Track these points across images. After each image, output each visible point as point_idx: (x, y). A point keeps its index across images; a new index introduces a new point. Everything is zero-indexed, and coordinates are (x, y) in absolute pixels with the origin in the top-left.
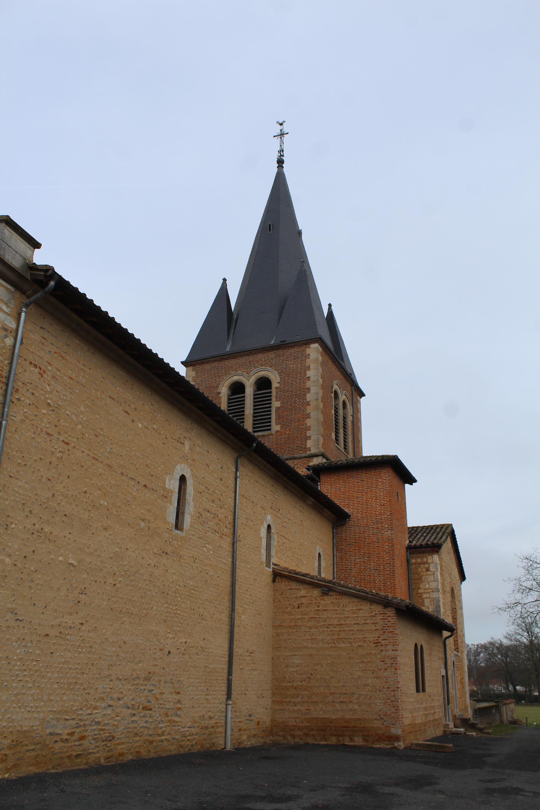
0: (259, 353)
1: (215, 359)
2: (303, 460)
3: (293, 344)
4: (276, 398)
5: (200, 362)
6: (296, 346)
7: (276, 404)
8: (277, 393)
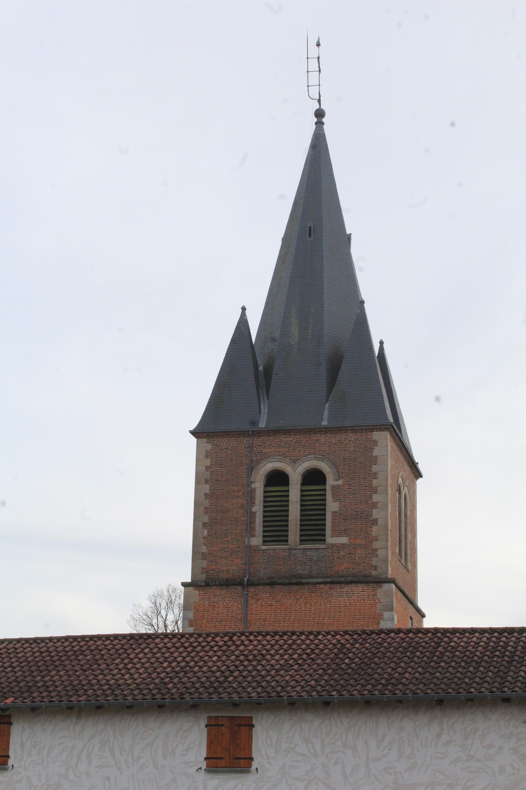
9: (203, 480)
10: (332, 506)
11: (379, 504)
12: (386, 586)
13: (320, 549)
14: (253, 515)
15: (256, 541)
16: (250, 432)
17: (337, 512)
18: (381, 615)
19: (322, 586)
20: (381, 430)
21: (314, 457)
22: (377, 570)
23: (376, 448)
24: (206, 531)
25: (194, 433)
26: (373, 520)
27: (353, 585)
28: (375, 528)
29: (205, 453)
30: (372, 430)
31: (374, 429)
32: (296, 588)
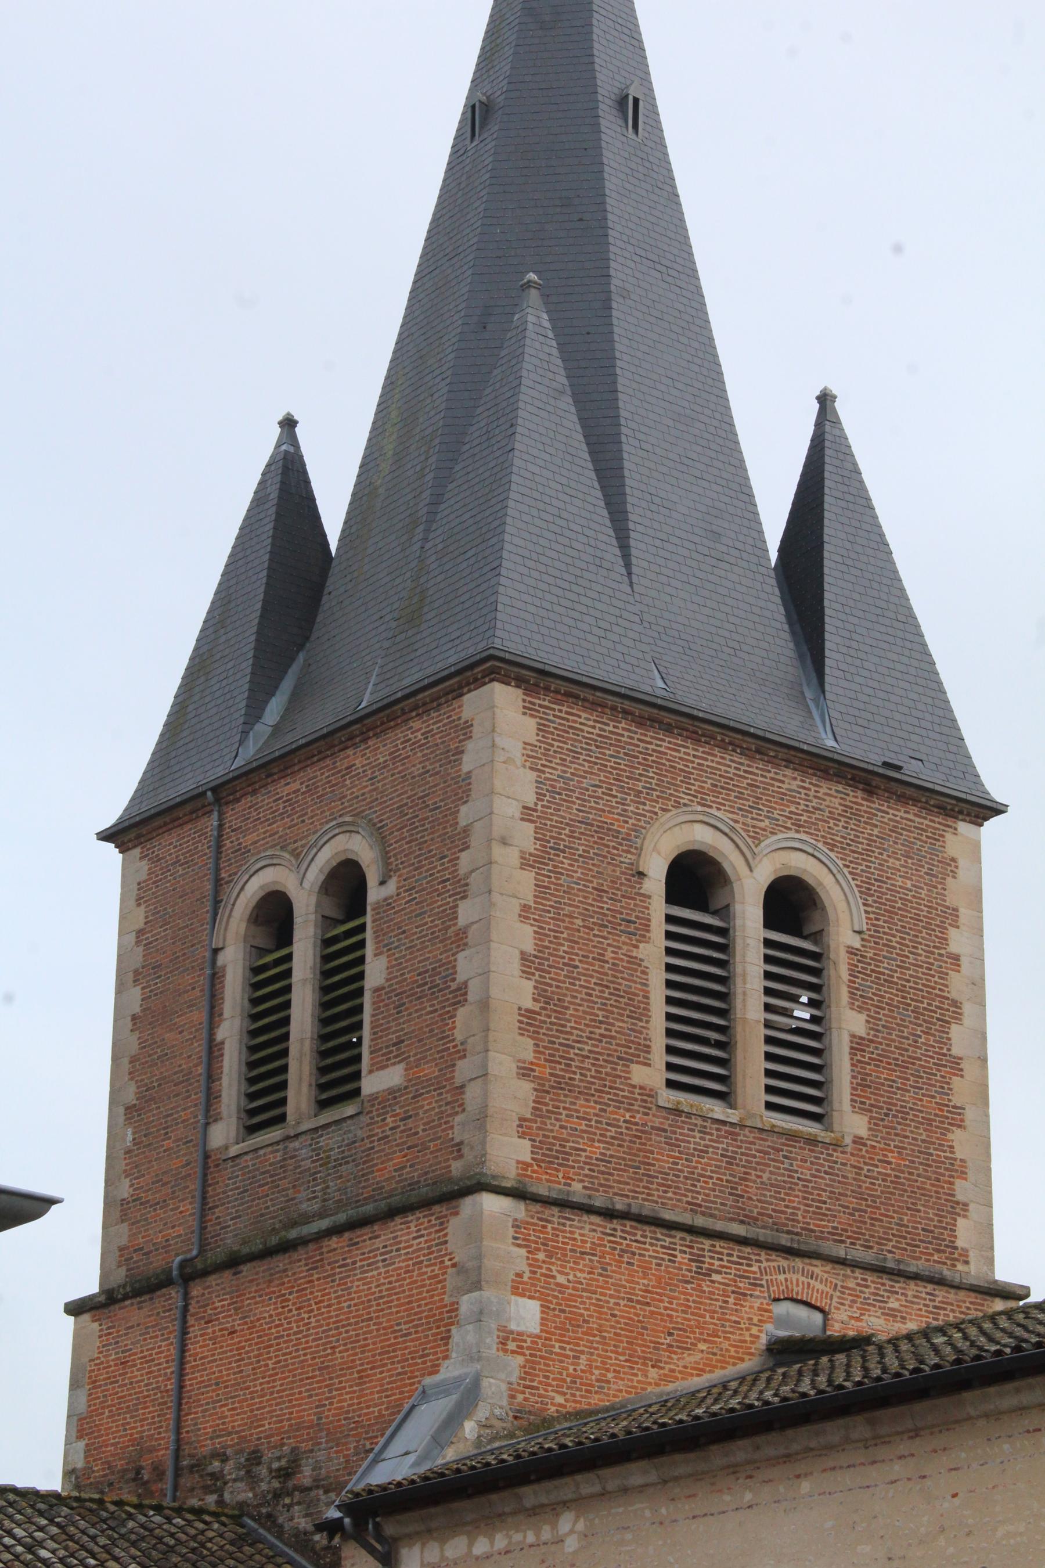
1: (627, 705)
2: (962, 1294)
3: (909, 792)
5: (564, 687)
6: (916, 801)
7: (849, 1022)
9: (131, 975)
10: (376, 971)
11: (471, 933)
12: (467, 1204)
13: (345, 1119)
14: (213, 1050)
15: (223, 1134)
16: (209, 793)
17: (383, 988)
18: (454, 1308)
19: (334, 1242)
20: (478, 683)
21: (339, 825)
22: (461, 1156)
23: (470, 745)
24: (130, 1131)
26: (459, 989)
27: (398, 1220)
28: (462, 1013)
29: (136, 892)
30: (457, 693)
31: (461, 687)
32: (280, 1262)
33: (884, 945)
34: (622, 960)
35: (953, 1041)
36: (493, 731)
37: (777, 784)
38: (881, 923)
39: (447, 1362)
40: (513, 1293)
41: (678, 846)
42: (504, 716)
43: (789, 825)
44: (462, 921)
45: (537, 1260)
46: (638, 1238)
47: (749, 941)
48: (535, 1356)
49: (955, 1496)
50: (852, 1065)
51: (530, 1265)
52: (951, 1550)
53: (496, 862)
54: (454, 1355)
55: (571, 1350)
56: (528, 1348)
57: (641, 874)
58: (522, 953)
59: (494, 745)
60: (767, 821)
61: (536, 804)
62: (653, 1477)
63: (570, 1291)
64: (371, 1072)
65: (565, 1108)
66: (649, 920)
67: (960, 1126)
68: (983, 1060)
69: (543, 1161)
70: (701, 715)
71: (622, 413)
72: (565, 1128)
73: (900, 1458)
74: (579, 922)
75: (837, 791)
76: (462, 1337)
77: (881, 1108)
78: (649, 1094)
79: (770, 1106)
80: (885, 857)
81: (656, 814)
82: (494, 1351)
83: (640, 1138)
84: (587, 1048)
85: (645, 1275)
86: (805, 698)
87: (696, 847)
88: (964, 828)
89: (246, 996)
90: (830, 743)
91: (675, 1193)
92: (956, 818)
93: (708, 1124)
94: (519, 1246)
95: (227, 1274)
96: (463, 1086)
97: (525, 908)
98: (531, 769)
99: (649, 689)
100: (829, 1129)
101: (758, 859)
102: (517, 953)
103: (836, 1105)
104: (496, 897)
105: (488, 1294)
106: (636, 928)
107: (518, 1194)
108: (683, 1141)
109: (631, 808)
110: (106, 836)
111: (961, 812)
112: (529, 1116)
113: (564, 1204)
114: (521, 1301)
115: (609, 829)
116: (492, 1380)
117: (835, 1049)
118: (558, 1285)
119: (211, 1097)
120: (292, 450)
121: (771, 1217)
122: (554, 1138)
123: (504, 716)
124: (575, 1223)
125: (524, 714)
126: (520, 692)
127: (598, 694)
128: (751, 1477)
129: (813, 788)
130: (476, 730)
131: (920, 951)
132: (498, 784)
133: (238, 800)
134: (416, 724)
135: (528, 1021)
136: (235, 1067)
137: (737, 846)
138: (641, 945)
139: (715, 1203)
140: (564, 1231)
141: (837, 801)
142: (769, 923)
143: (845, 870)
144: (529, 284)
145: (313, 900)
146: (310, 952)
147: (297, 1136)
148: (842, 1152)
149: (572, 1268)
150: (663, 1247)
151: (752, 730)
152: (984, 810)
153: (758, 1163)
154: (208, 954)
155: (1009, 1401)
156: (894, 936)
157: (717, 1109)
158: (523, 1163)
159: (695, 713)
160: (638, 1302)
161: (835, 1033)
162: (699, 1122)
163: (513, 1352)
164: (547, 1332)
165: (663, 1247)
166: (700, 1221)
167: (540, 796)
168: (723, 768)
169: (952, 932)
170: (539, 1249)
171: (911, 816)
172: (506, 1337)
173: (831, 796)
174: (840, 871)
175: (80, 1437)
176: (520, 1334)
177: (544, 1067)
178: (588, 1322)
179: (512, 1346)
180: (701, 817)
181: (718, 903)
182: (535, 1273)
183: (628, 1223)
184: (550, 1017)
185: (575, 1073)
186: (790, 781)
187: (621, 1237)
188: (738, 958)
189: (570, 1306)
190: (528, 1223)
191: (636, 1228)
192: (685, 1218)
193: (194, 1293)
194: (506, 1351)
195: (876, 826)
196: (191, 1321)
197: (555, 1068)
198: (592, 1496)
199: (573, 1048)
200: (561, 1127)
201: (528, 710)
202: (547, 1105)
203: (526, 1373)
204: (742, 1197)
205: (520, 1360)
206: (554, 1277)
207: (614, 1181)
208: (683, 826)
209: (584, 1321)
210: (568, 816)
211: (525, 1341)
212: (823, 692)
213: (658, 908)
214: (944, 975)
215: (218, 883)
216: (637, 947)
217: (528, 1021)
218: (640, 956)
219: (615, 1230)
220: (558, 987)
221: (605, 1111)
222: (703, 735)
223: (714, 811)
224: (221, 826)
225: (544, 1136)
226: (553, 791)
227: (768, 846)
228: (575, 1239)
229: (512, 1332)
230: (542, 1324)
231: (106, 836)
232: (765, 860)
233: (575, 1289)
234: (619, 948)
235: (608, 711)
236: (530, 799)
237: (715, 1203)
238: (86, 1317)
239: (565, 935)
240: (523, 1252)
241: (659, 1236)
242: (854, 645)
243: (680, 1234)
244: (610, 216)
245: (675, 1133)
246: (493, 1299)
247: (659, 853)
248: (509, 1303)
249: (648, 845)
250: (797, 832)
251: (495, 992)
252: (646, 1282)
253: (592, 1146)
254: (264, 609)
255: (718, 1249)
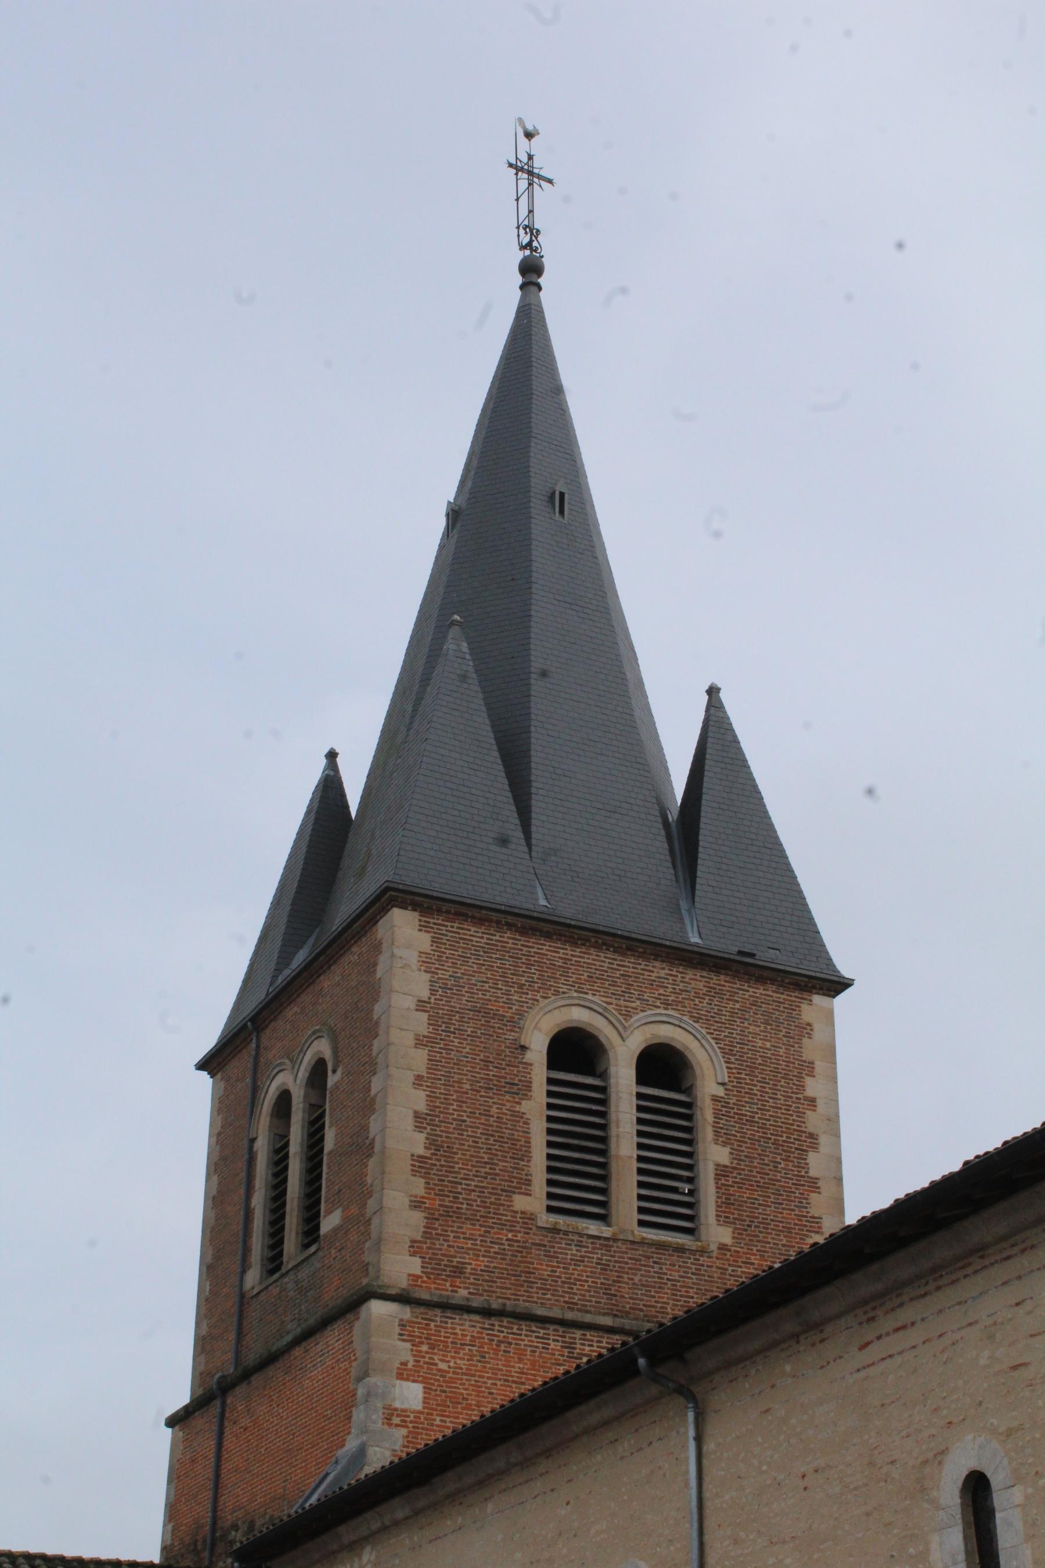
0: (657, 957)
1: (510, 919)
3: (765, 974)
4: (717, 1133)
6: (773, 981)
7: (713, 1153)
8: (716, 1116)
15: (252, 1277)
16: (249, 1024)
19: (297, 1352)
20: (385, 910)
25: (209, 1064)
30: (374, 921)
31: (376, 916)
32: (271, 1371)
33: (746, 1093)
34: (506, 1114)
35: (810, 1165)
36: (393, 944)
37: (647, 973)
38: (743, 1076)
39: (350, 1437)
40: (398, 1378)
41: (558, 1025)
42: (404, 932)
43: (658, 1004)
44: (373, 1092)
45: (420, 1351)
46: (515, 1331)
47: (621, 1095)
48: (418, 1428)
49: (568, 1503)
50: (717, 1188)
51: (414, 1356)
52: (565, 1551)
53: (393, 1044)
54: (353, 1431)
55: (451, 1422)
56: (411, 1422)
57: (524, 1048)
58: (415, 1112)
59: (393, 955)
60: (638, 1003)
61: (430, 998)
62: (407, 1511)
63: (451, 1375)
64: (325, 1217)
65: (452, 1231)
66: (531, 1082)
67: (818, 1233)
68: (839, 1180)
69: (432, 1274)
70: (573, 923)
71: (533, 711)
72: (453, 1247)
73: (541, 1475)
74: (467, 1086)
75: (701, 976)
76: (358, 1415)
77: (744, 1221)
78: (529, 1218)
79: (642, 1223)
80: (746, 1025)
81: (537, 1001)
82: (379, 1425)
83: (521, 1252)
84: (473, 1183)
85: (520, 1360)
86: (679, 909)
87: (574, 1025)
88: (818, 999)
89: (270, 1172)
90: (695, 939)
91: (553, 1295)
92: (811, 992)
93: (584, 1239)
94: (404, 1340)
95: (244, 1386)
96: (370, 1219)
97: (419, 1077)
98: (426, 971)
99: (531, 907)
100: (698, 1240)
101: (629, 1031)
102: (411, 1112)
103: (703, 1220)
104: (393, 1071)
105: (371, 1380)
106: (519, 1089)
107: (403, 1298)
108: (561, 1253)
109: (515, 998)
110: (202, 1066)
111: (814, 987)
112: (419, 1238)
113: (445, 1306)
114: (405, 1384)
115: (494, 1014)
116: (377, 1449)
117: (702, 1176)
118: (439, 1370)
119: (246, 1251)
120: (332, 773)
121: (642, 1310)
122: (443, 1255)
123: (404, 932)
124: (457, 1321)
125: (420, 930)
126: (416, 914)
127: (483, 912)
128: (461, 1504)
129: (680, 975)
130: (385, 945)
131: (779, 1096)
132: (396, 984)
133: (267, 1026)
134: (354, 949)
135: (420, 1165)
136: (261, 1225)
137: (610, 1022)
138: (524, 1102)
139: (590, 1301)
140: (447, 1328)
141: (701, 984)
142: (641, 1080)
143: (708, 1037)
144: (453, 623)
145: (302, 1092)
146: (299, 1132)
147: (287, 1272)
148: (708, 1257)
149: (453, 1357)
150: (537, 1337)
151: (619, 932)
152: (837, 985)
153: (630, 1268)
154: (245, 1143)
155: (594, 1419)
156: (755, 1086)
157: (593, 1228)
158: (413, 1275)
159: (597, 928)
160: (514, 1382)
161: (701, 1163)
162: (576, 1238)
163: (397, 1425)
164: (429, 1409)
165: (537, 1337)
166: (570, 1316)
167: (433, 991)
168: (598, 963)
169: (809, 1081)
170: (422, 1343)
171: (769, 993)
172: (390, 1414)
173: (696, 980)
174: (704, 1037)
175: (170, 1521)
176: (403, 1410)
177: (434, 1199)
178: (467, 1399)
179: (396, 1420)
180: (577, 1002)
181: (600, 1069)
182: (418, 1361)
183: (505, 1320)
184: (439, 1160)
185: (462, 1203)
186: (659, 970)
187: (499, 1331)
188: (613, 1108)
189: (450, 1387)
190: (413, 1322)
191: (513, 1323)
192: (556, 1313)
193: (229, 1401)
194: (390, 1425)
195: (738, 1002)
196: (226, 1423)
197: (443, 1201)
198: (379, 1531)
199: (461, 1184)
200: (449, 1246)
201: (423, 927)
202: (436, 1229)
203: (408, 1442)
204: (615, 1295)
205: (404, 1431)
206: (436, 1364)
207: (497, 1287)
208: (562, 1009)
209: (464, 1399)
210: (458, 1006)
211: (408, 1416)
212: (694, 902)
213: (539, 1073)
214: (801, 1114)
215: (255, 1090)
216: (520, 1103)
217: (420, 1165)
218: (523, 1110)
219: (493, 1325)
220: (447, 1137)
221: (489, 1232)
222: (579, 939)
223: (590, 997)
224: (258, 1047)
225: (433, 1254)
226: (445, 987)
227: (639, 1020)
228: (455, 1334)
229: (396, 1410)
230: (424, 1403)
231: (202, 1066)
232: (636, 1032)
233: (454, 1373)
234: (504, 1105)
235: (494, 924)
236: (425, 994)
237: (590, 1301)
238: (177, 1428)
239: (454, 1097)
240: (408, 1345)
241: (534, 1328)
242: (724, 867)
243: (552, 1327)
244: (534, 574)
245: (553, 1247)
246: (379, 1383)
247: (540, 1030)
248: (394, 1386)
249: (529, 1023)
250: (665, 1009)
251: (390, 1143)
252: (521, 1366)
253: (477, 1260)
254: (299, 887)
255: (588, 1337)
